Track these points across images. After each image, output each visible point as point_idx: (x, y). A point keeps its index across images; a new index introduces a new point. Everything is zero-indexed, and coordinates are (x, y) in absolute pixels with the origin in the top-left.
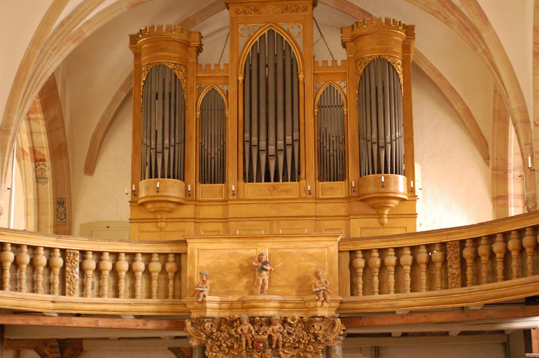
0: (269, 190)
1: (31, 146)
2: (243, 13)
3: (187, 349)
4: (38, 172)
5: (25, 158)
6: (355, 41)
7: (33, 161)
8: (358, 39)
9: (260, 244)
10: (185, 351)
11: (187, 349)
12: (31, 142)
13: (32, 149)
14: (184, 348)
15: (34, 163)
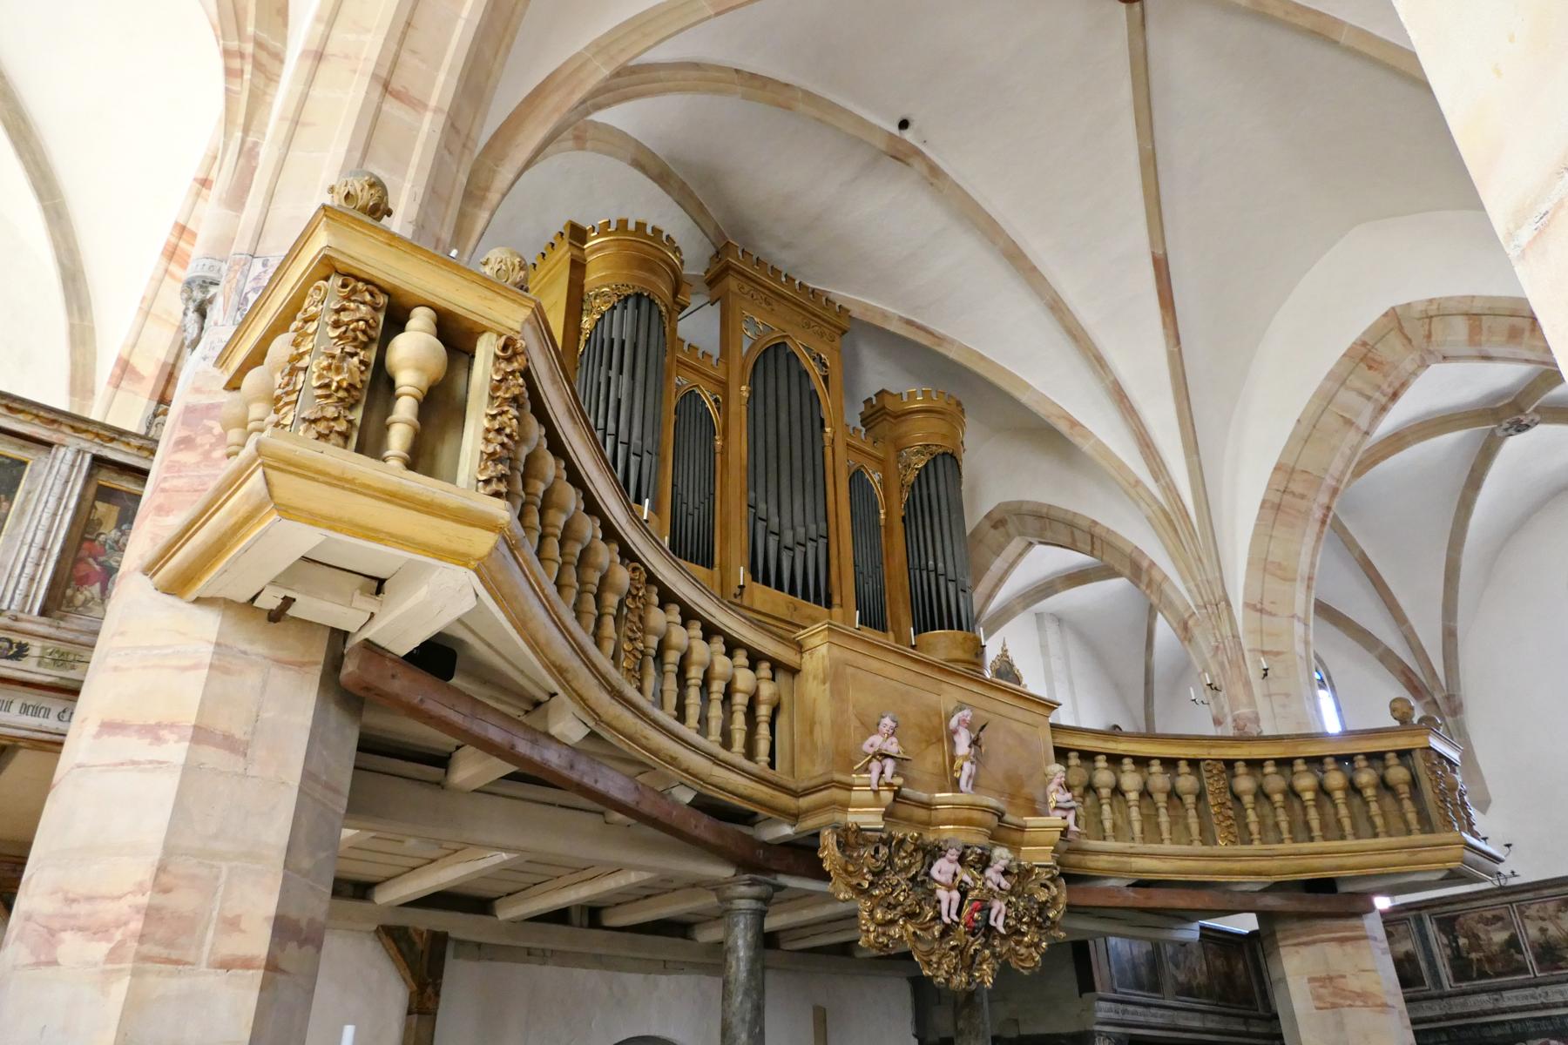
0: (788, 607)
1: (171, 361)
2: (749, 297)
3: (422, 934)
4: (154, 429)
5: (123, 384)
6: (899, 419)
7: (157, 398)
8: (903, 418)
9: (945, 686)
10: (417, 939)
11: (422, 934)
12: (175, 351)
13: (169, 369)
14: (416, 930)
15: (154, 404)
